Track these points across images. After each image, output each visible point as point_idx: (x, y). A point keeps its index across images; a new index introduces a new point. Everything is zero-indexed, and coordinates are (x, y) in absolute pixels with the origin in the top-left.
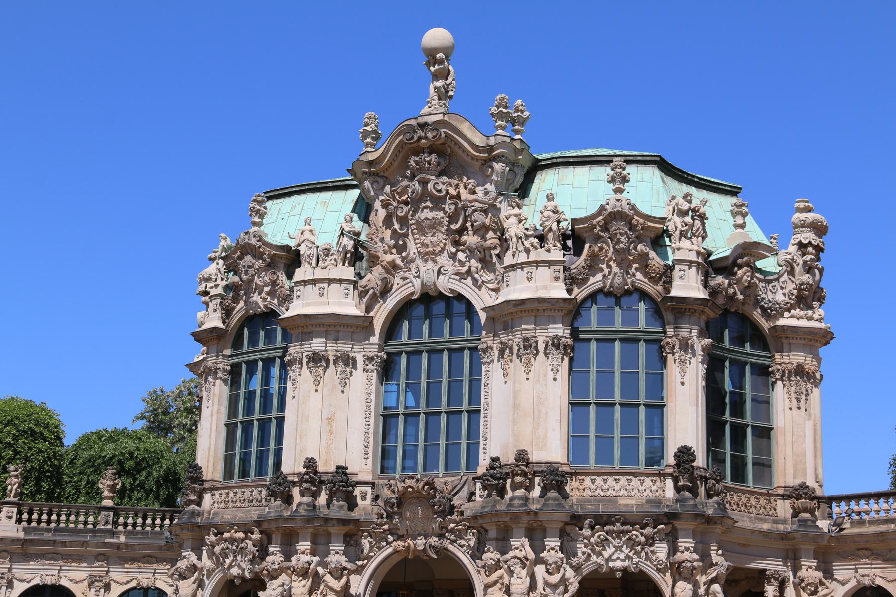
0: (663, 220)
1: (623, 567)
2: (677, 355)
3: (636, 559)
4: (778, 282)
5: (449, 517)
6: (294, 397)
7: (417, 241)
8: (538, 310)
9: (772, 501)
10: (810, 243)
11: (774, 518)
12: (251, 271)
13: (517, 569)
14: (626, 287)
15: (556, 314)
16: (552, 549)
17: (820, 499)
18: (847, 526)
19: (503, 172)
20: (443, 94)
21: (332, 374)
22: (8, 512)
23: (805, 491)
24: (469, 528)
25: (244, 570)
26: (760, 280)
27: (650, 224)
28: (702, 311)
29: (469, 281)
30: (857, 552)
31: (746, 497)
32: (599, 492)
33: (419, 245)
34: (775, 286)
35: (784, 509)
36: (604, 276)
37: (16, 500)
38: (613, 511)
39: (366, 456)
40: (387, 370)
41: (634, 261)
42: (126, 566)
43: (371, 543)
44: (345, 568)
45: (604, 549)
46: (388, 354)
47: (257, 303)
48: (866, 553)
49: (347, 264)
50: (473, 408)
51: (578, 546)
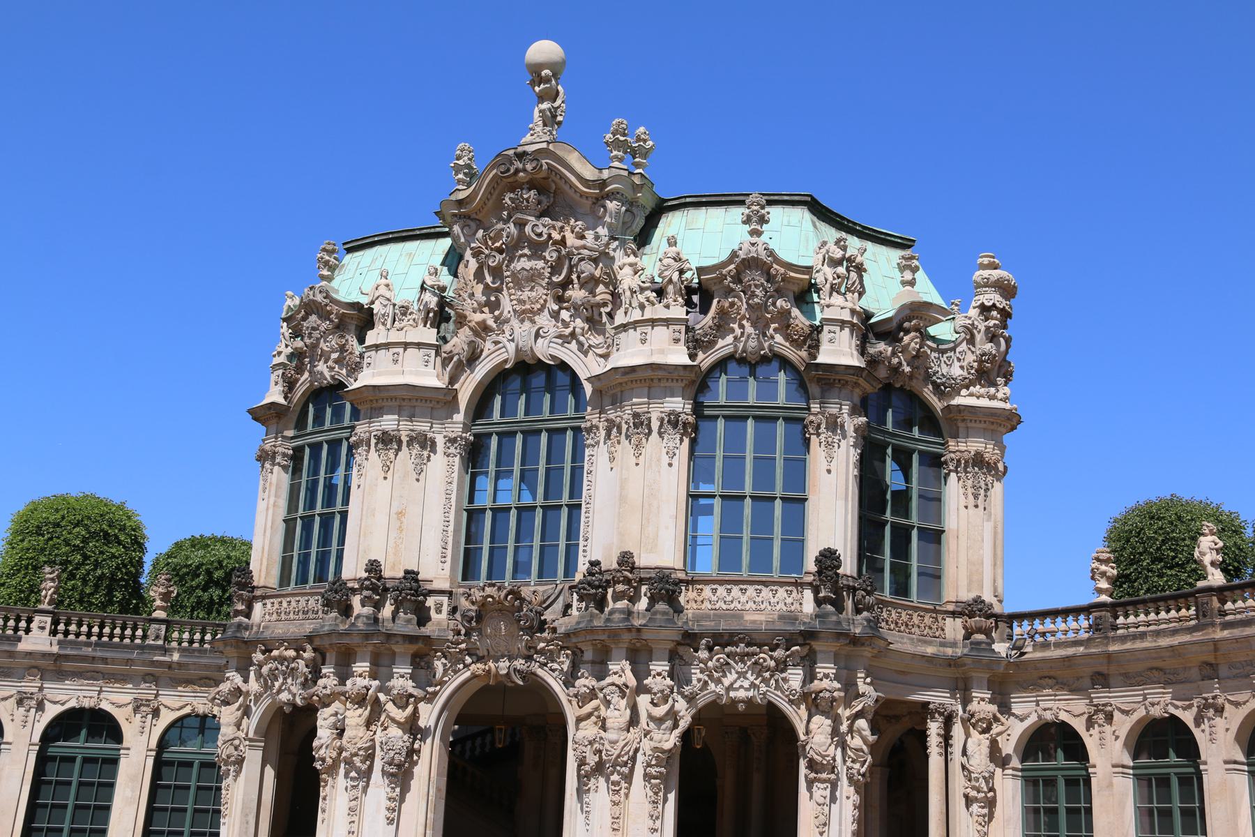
0: (808, 270)
1: (747, 698)
2: (822, 437)
3: (763, 688)
4: (955, 352)
5: (539, 635)
6: (359, 486)
7: (512, 297)
8: (652, 380)
9: (940, 619)
10: (994, 305)
11: (941, 640)
12: (316, 334)
13: (615, 699)
14: (762, 352)
15: (674, 384)
16: (659, 674)
17: (998, 617)
18: (1029, 649)
19: (618, 213)
20: (550, 119)
21: (405, 461)
22: (41, 622)
23: (979, 607)
24: (562, 648)
25: (294, 695)
26: (932, 350)
27: (792, 274)
28: (856, 383)
29: (574, 345)
30: (1039, 681)
31: (907, 614)
32: (721, 604)
33: (515, 302)
34: (951, 357)
35: (954, 628)
36: (735, 338)
37: (50, 608)
38: (737, 628)
39: (443, 560)
40: (474, 455)
41: (773, 320)
42: (179, 688)
43: (445, 665)
44: (411, 696)
45: (725, 676)
46: (475, 435)
47: (322, 373)
48: (1050, 682)
49: (428, 326)
50: (574, 501)
51: (693, 671)
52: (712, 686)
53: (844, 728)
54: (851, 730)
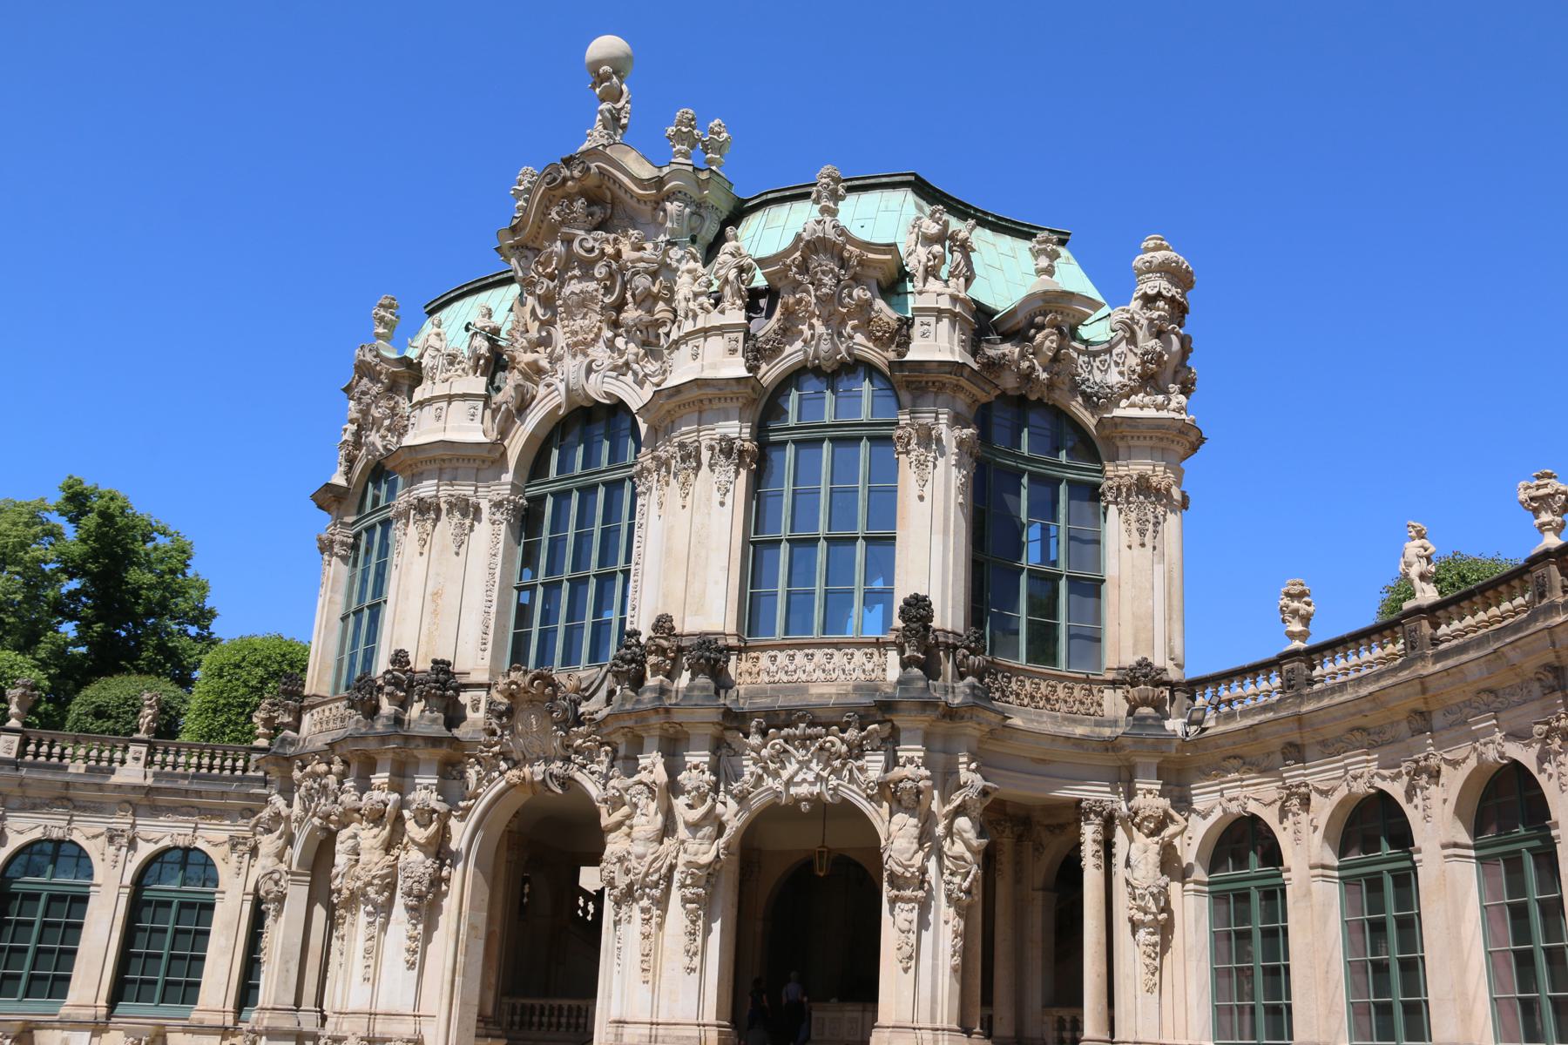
0: (891, 248)
1: (812, 794)
2: (913, 455)
3: (833, 781)
4: (1111, 355)
5: (575, 729)
8: (701, 401)
9: (1095, 691)
10: (1159, 294)
11: (1098, 718)
12: (366, 399)
14: (838, 357)
15: (729, 405)
16: (696, 767)
17: (1173, 686)
18: (1211, 723)
19: (680, 215)
21: (447, 526)
23: (1144, 671)
24: (602, 744)
26: (1080, 352)
27: (871, 256)
28: (957, 386)
29: (629, 377)
30: (1223, 763)
31: (1048, 685)
34: (1106, 361)
35: (1114, 703)
40: (526, 521)
41: (850, 315)
43: (478, 773)
44: (434, 811)
45: (783, 767)
46: (528, 499)
47: (373, 444)
48: (1236, 763)
49: (478, 374)
51: (745, 763)
52: (769, 782)
53: (940, 830)
54: (949, 832)
